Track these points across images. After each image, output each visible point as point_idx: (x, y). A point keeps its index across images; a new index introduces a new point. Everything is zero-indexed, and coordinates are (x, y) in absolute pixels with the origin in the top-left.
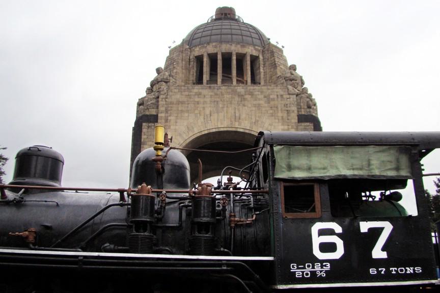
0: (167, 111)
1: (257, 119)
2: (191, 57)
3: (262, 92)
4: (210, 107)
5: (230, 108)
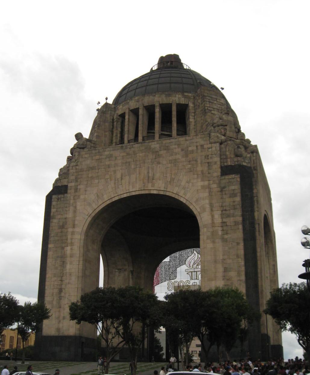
0: (76, 180)
1: (173, 176)
2: (115, 117)
3: (179, 145)
5: (143, 168)
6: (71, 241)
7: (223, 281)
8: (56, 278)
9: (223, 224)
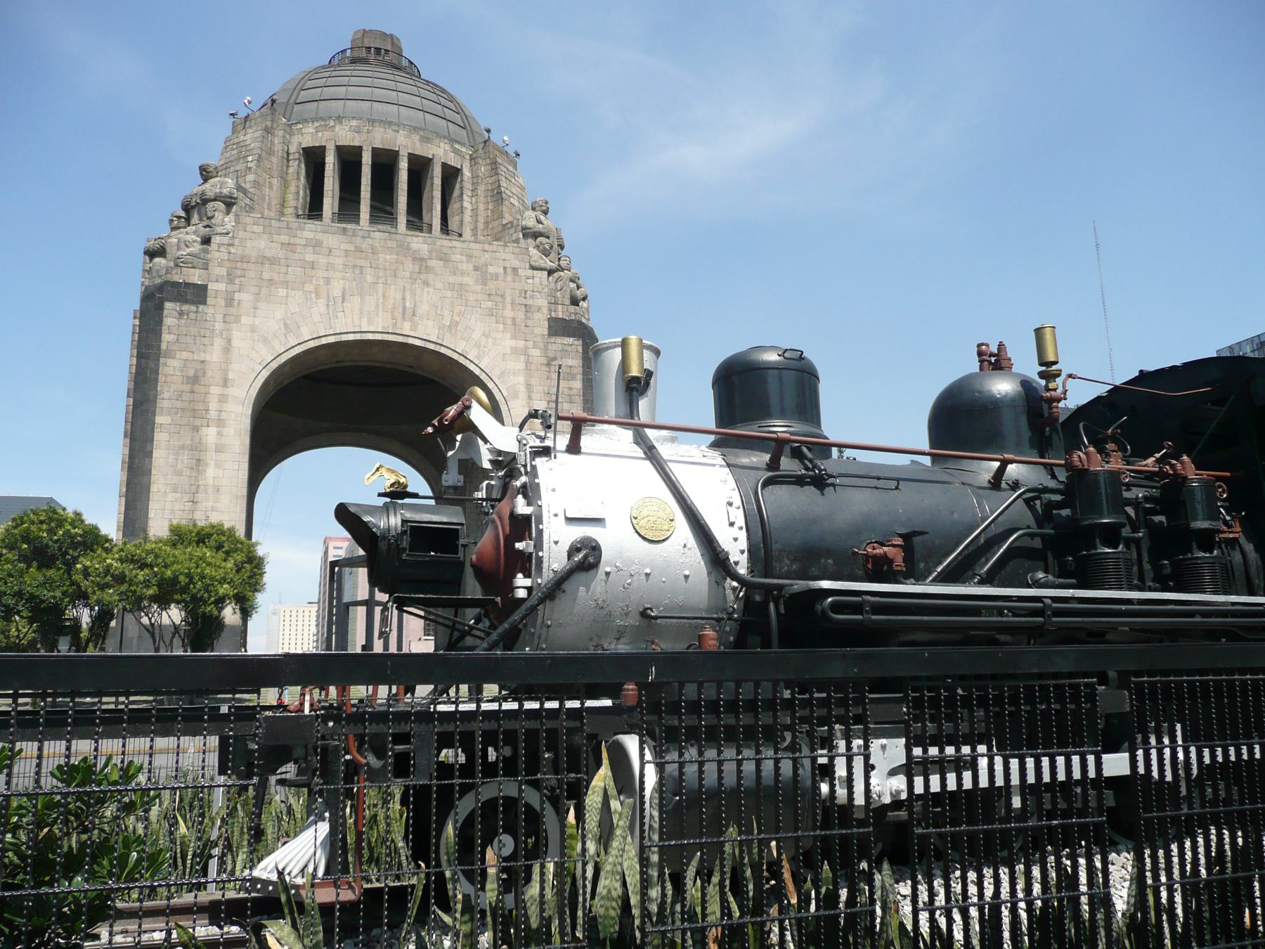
0: (230, 278)
1: (456, 318)
2: (293, 149)
3: (469, 257)
5: (393, 287)
8: (178, 495)
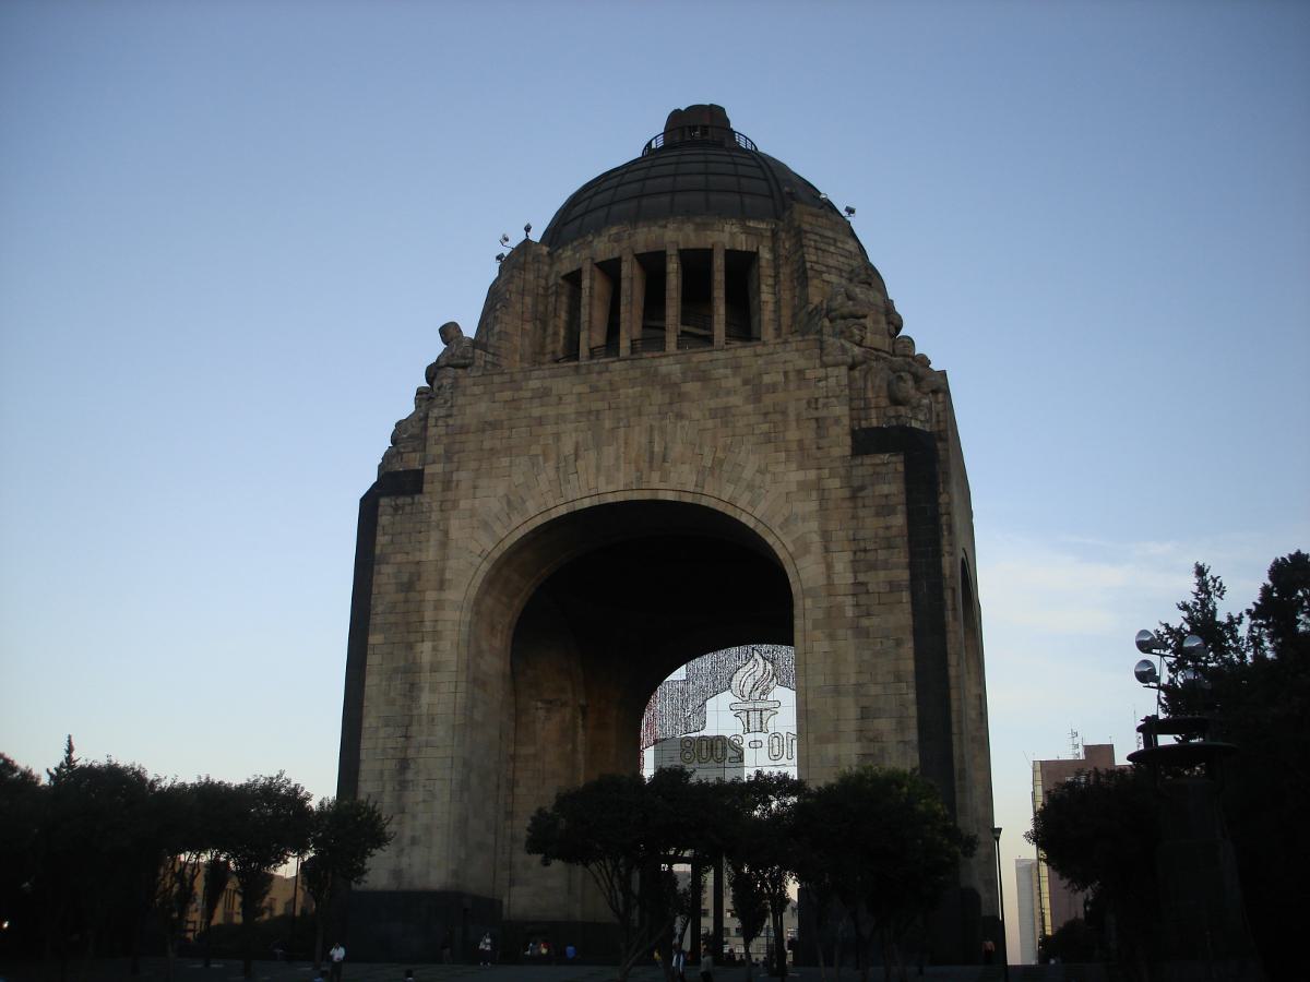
0: (448, 456)
1: (720, 455)
3: (737, 368)
4: (576, 431)
5: (637, 428)
6: (434, 627)
7: (858, 744)
8: (390, 730)
9: (859, 588)
